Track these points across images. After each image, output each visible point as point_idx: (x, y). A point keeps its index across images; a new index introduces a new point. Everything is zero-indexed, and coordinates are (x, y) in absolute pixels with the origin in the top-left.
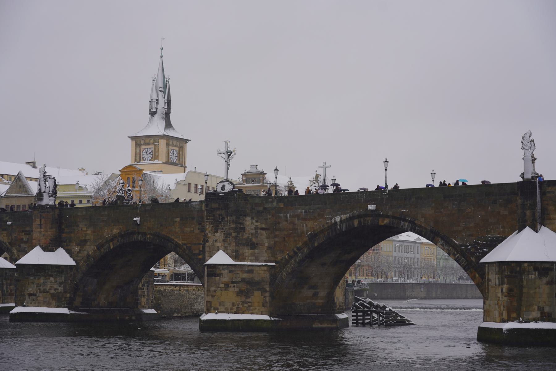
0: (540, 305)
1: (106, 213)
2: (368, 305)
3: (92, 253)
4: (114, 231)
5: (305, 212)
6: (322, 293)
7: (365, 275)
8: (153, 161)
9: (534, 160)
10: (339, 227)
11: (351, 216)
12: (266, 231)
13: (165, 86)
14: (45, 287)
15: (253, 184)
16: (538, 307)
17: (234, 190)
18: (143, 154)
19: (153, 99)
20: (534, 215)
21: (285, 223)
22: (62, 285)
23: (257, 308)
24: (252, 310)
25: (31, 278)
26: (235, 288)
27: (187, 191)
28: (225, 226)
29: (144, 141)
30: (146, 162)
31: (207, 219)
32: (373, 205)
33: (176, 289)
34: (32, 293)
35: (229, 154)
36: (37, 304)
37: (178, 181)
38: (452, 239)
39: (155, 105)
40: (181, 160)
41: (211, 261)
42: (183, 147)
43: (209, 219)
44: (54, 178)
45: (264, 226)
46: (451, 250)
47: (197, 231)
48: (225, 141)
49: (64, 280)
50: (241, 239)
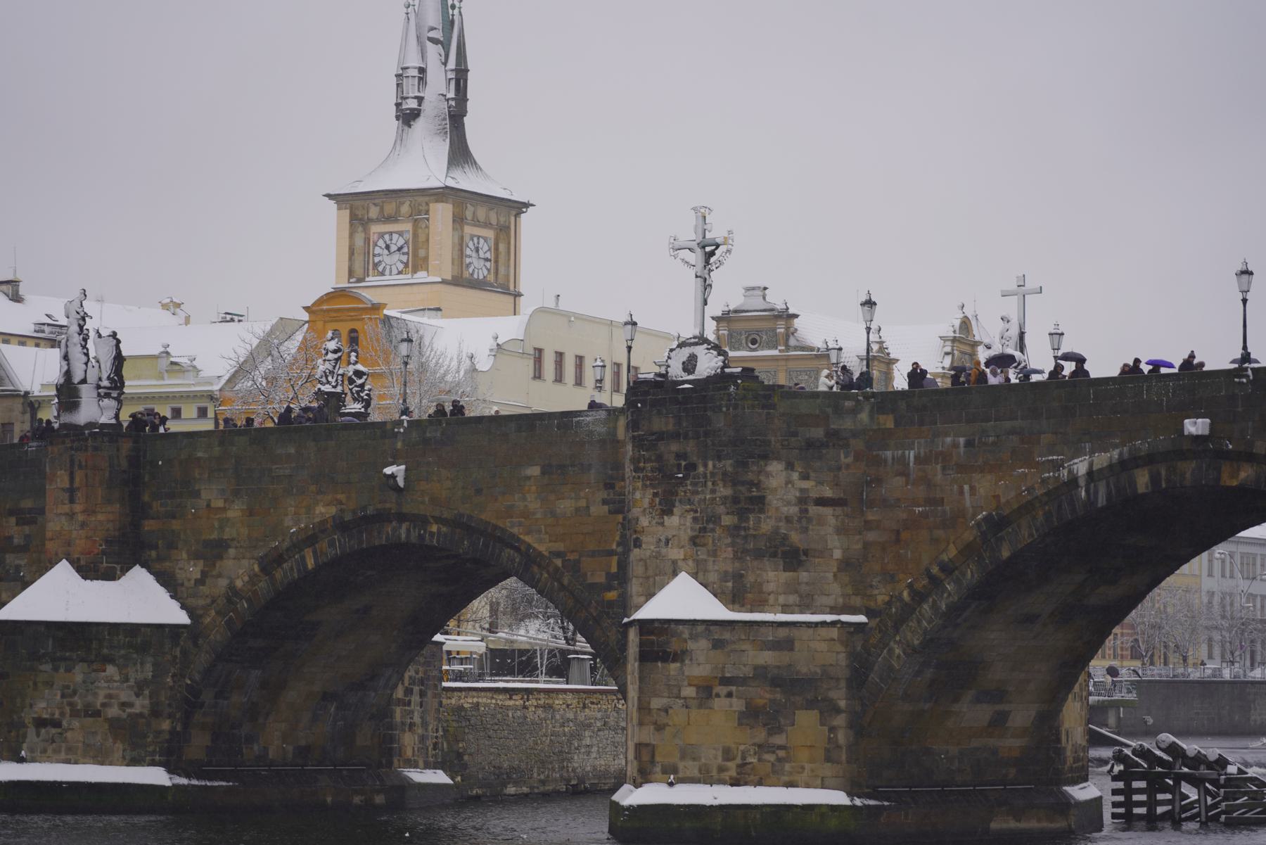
1: (292, 451)
2: (1165, 757)
4: (317, 512)
5: (969, 444)
6: (1022, 715)
7: (1109, 655)
8: (409, 276)
10: (1083, 493)
11: (1126, 456)
12: (834, 510)
13: (449, 24)
14: (90, 698)
17: (727, 370)
18: (376, 252)
19: (407, 68)
21: (900, 481)
22: (147, 692)
23: (807, 766)
24: (790, 773)
25: (43, 667)
26: (734, 700)
27: (532, 374)
29: (378, 207)
30: (387, 279)
31: (637, 470)
32: (1200, 420)
33: (511, 703)
34: (45, 716)
35: (709, 251)
37: (500, 341)
40: (502, 270)
41: (651, 610)
43: (643, 469)
44: (114, 335)
45: (828, 492)
47: (599, 510)
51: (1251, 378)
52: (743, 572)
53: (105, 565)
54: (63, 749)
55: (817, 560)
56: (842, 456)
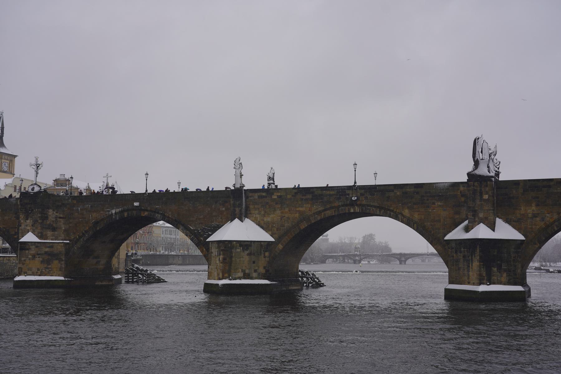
2: (136, 270)
5: (91, 207)
6: (103, 261)
9: (241, 176)
11: (123, 210)
15: (61, 187)
16: (242, 270)
17: (41, 190)
20: (241, 210)
21: (76, 214)
26: (40, 258)
27: (14, 191)
28: (33, 216)
32: (137, 203)
35: (38, 166)
40: (10, 169)
41: (22, 240)
43: (22, 211)
45: (61, 216)
48: (35, 157)
56: (65, 208)
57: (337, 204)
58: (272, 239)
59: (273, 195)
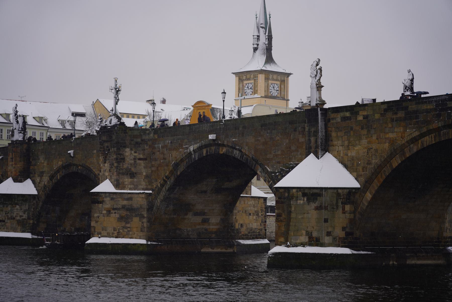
0: (309, 229)
3: (47, 183)
4: (59, 163)
5: (171, 143)
9: (319, 87)
10: (193, 156)
11: (200, 145)
12: (143, 161)
14: (12, 214)
16: (307, 231)
18: (245, 89)
20: (316, 141)
21: (158, 153)
22: (26, 213)
26: (116, 214)
28: (110, 157)
32: (212, 135)
36: (5, 229)
38: (266, 166)
39: (257, 41)
40: (283, 93)
42: (284, 81)
45: (141, 156)
46: (267, 177)
48: (115, 78)
49: (27, 208)
50: (121, 169)
51: (224, 123)
52: (119, 179)
53: (19, 178)
54: (5, 228)
55: (139, 175)
57: (436, 124)
58: (355, 184)
59: (358, 114)
